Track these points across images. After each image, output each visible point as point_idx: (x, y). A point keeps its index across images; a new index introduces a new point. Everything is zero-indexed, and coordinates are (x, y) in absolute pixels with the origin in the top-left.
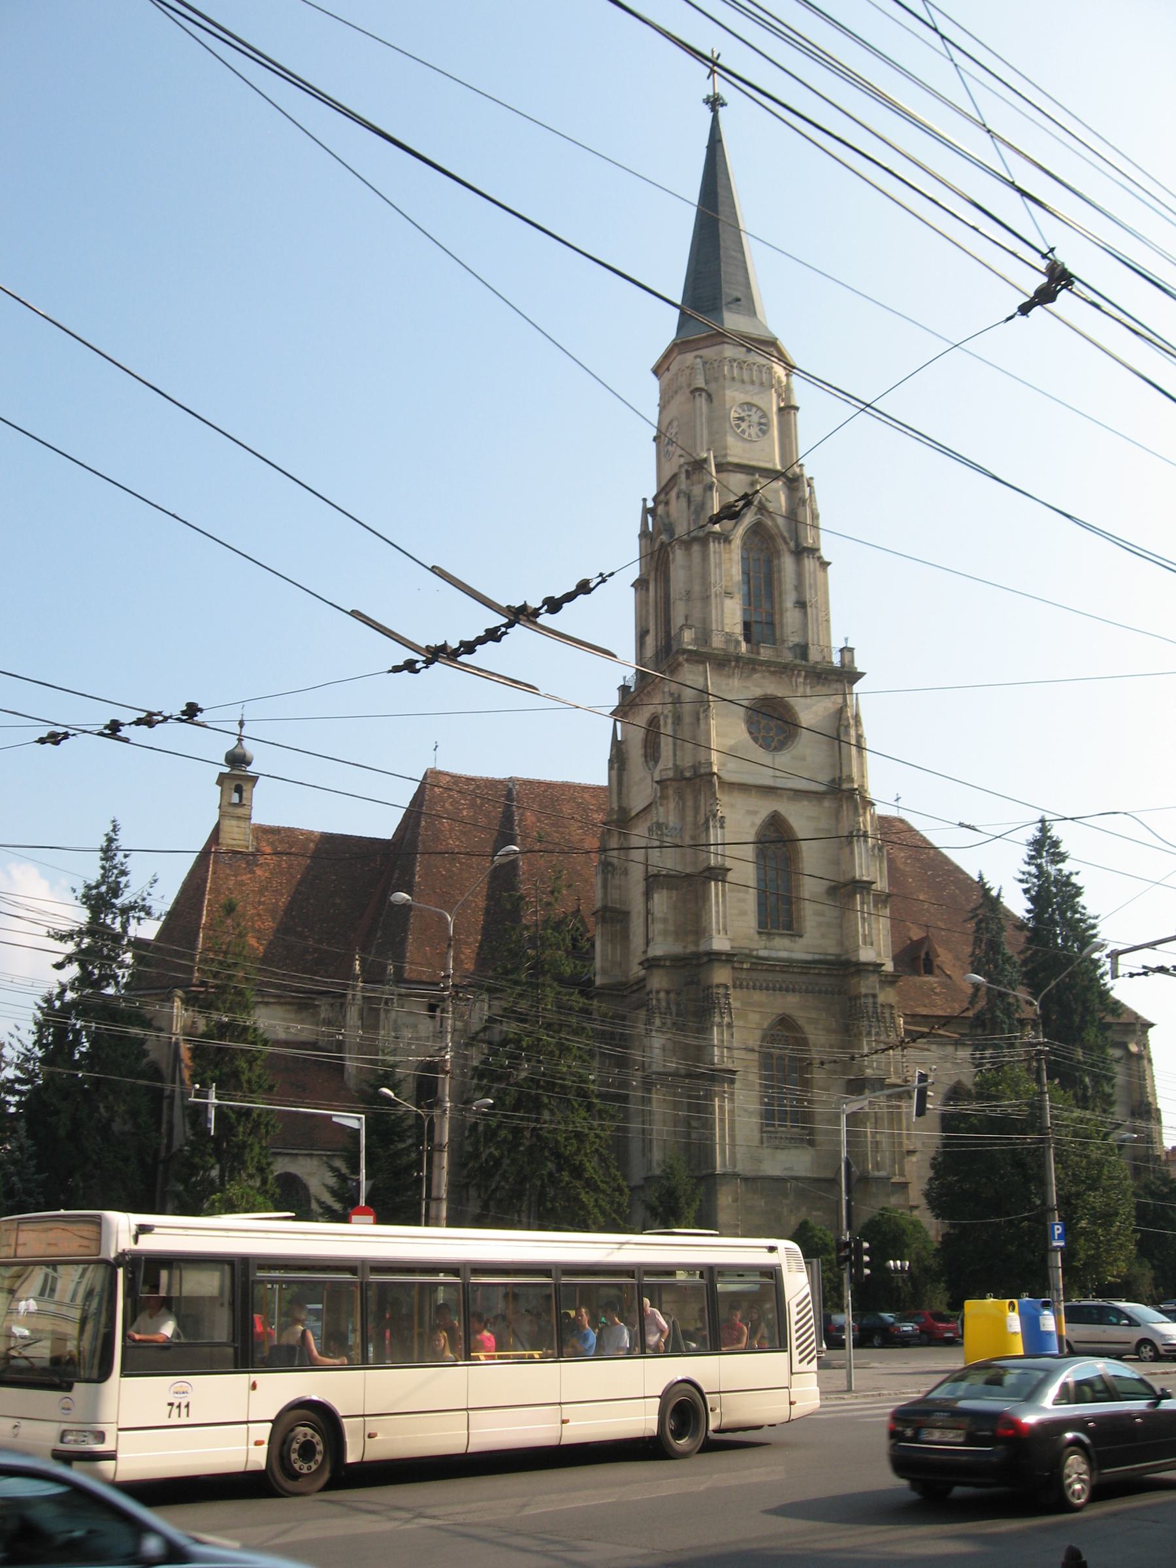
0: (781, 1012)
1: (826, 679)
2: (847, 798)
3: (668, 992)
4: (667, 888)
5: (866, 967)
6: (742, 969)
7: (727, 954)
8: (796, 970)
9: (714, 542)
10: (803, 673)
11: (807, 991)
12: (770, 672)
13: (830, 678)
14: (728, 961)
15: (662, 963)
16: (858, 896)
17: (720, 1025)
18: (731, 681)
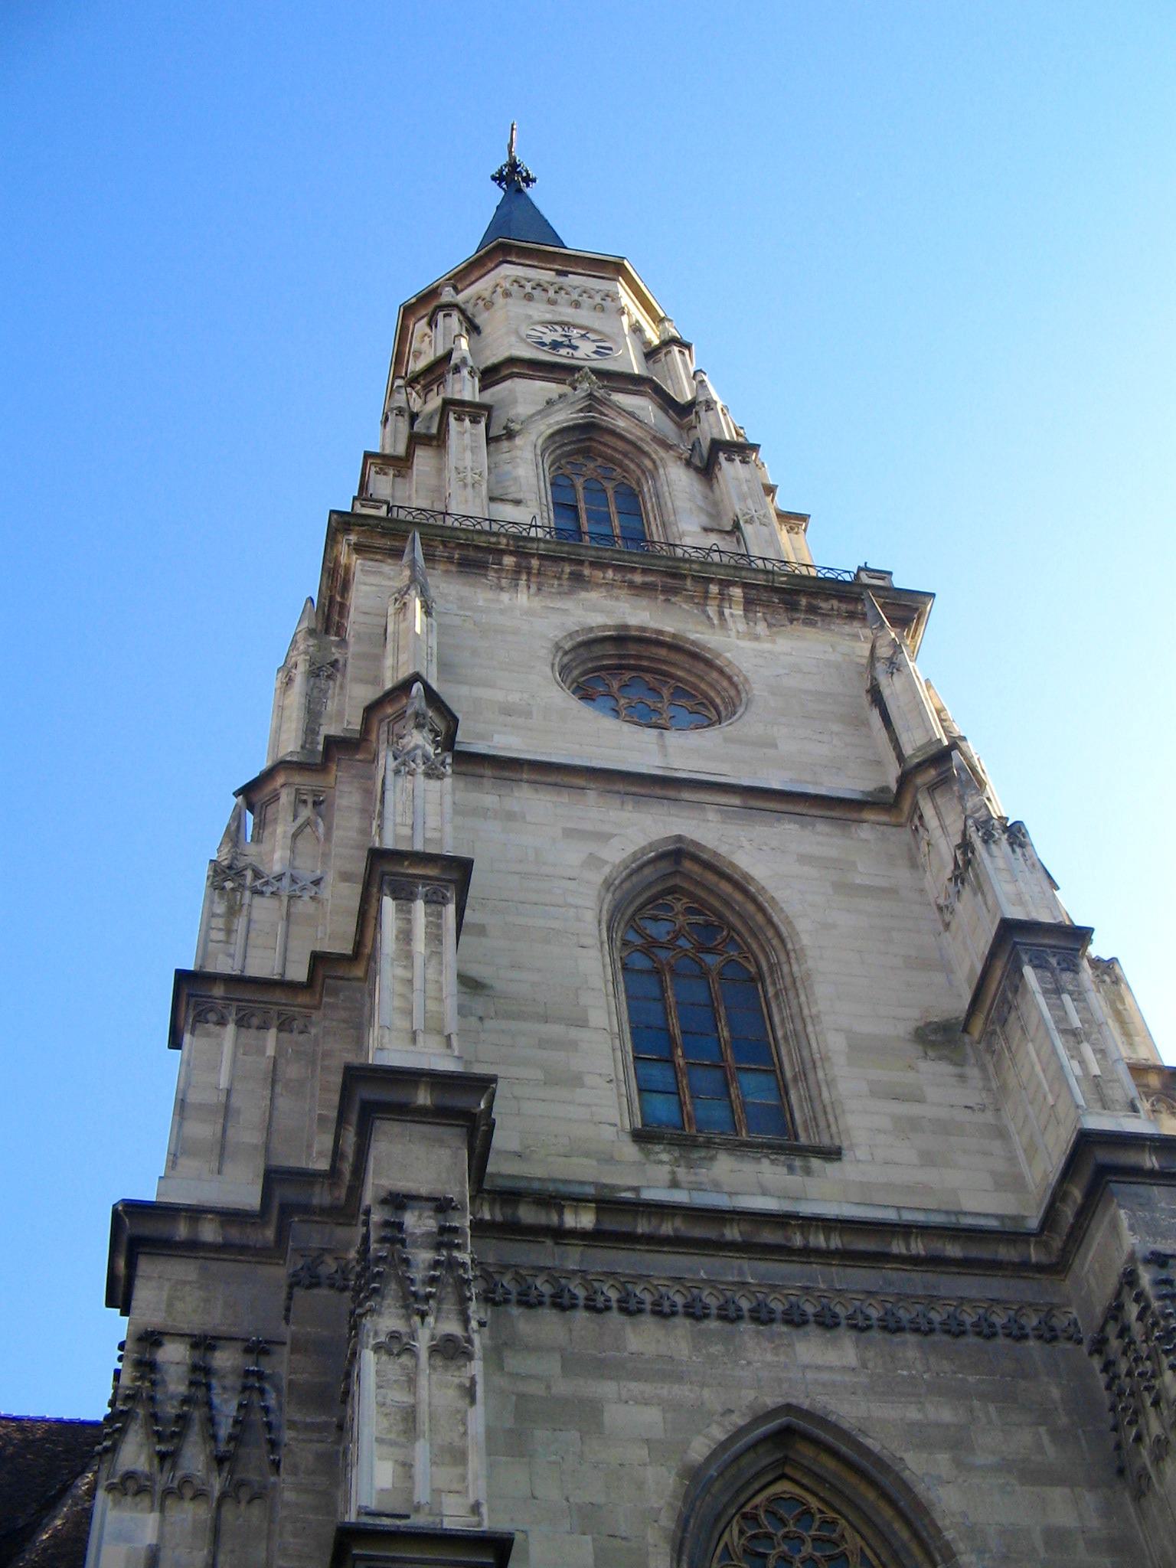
0: (771, 1401)
1: (812, 610)
2: (932, 788)
3: (203, 1343)
4: (241, 1023)
5: (1130, 1158)
6: (561, 1235)
7: (438, 1080)
8: (819, 1240)
9: (459, 419)
10: (737, 592)
11: (892, 1327)
12: (632, 585)
13: (824, 605)
14: (440, 1115)
15: (182, 1231)
16: (1028, 971)
17: (397, 1345)
18: (505, 597)
